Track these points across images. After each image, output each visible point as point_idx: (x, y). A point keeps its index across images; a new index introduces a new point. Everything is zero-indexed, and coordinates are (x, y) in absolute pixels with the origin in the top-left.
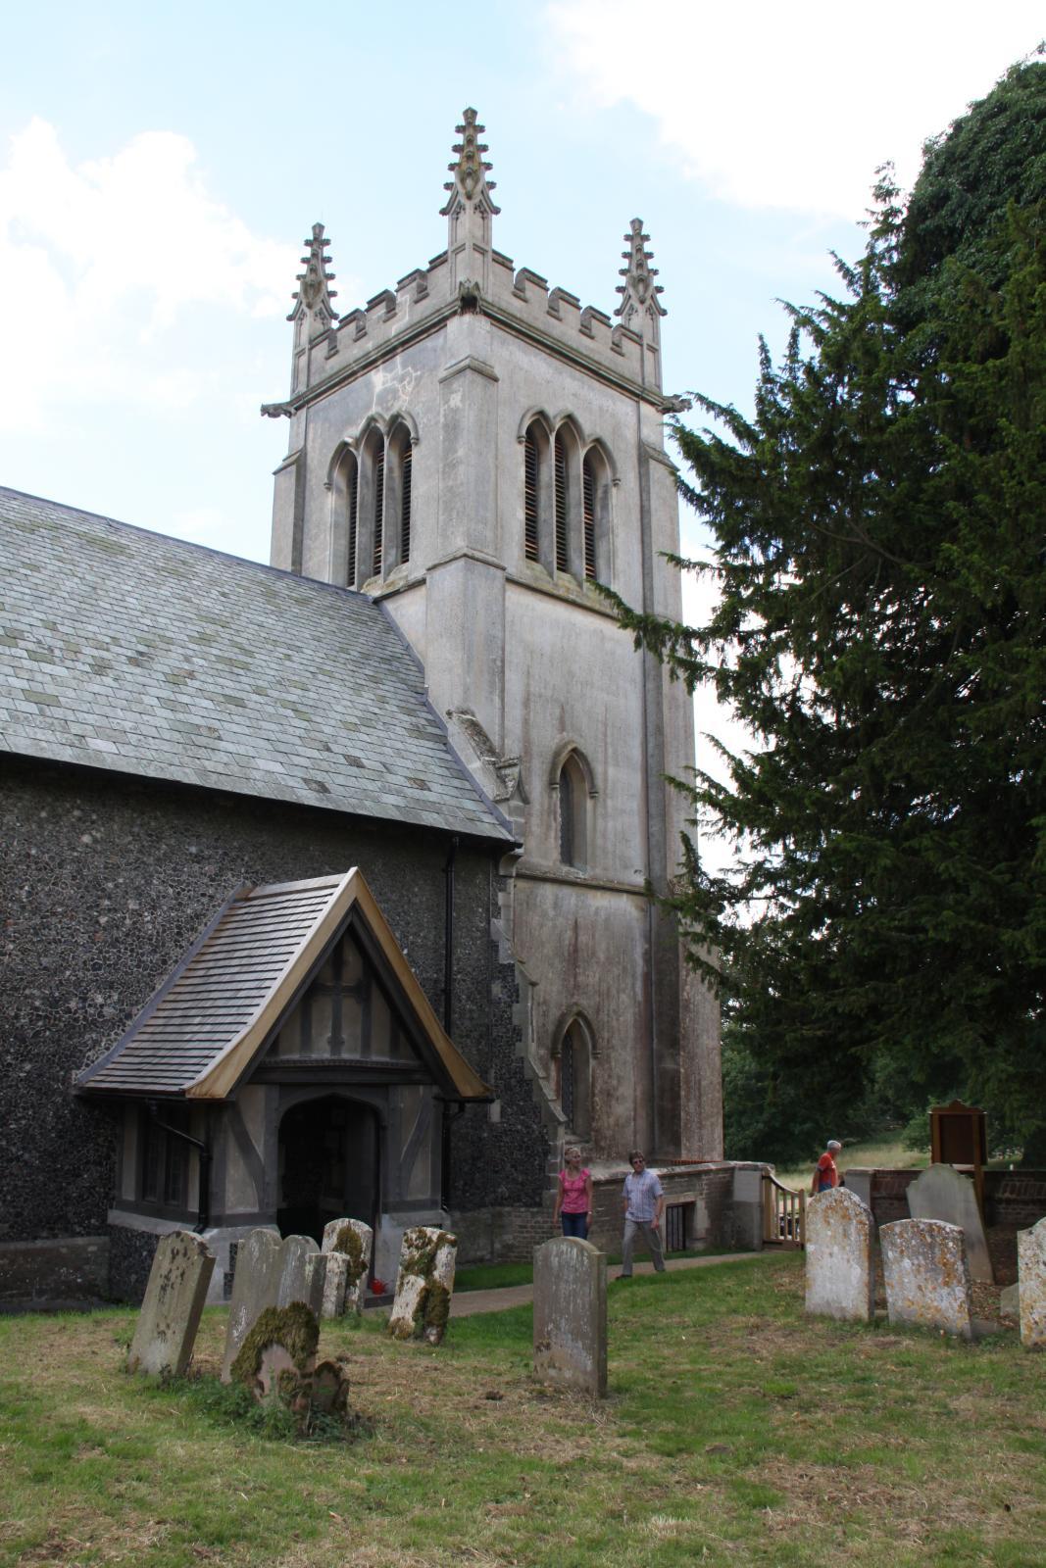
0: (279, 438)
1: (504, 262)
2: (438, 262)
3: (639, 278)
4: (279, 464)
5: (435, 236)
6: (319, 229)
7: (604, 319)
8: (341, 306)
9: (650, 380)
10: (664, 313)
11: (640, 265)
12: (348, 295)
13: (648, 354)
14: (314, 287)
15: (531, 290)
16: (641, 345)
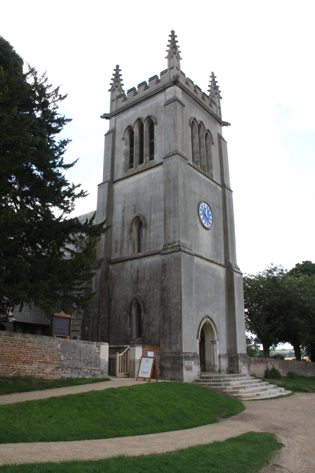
0: (106, 125)
2: (162, 73)
3: (214, 87)
4: (106, 132)
5: (164, 65)
9: (219, 116)
10: (221, 98)
11: (215, 84)
16: (216, 106)
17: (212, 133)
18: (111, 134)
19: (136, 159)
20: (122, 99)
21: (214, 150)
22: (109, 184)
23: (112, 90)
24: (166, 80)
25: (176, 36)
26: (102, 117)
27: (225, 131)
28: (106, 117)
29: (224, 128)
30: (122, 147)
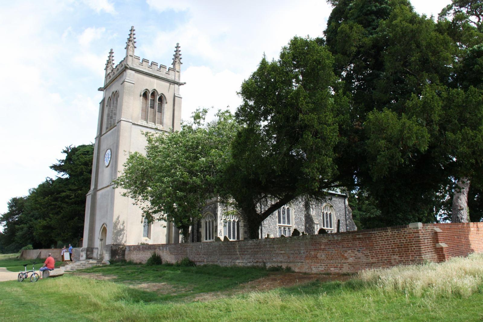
0: (101, 96)
1: (138, 58)
6: (112, 50)
13: (177, 74)
17: (165, 95)
20: (108, 77)
21: (167, 108)
27: (182, 91)
28: (100, 89)
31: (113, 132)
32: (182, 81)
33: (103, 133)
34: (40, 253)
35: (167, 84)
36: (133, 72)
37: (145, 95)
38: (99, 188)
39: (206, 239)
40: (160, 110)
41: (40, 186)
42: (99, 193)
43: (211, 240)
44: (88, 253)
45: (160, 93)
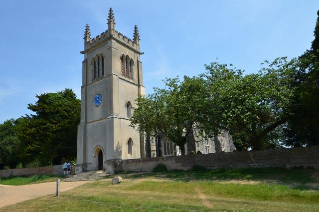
0: (82, 57)
7: (131, 40)
8: (92, 37)
12: (93, 35)
14: (87, 33)
15: (120, 36)
18: (85, 62)
19: (97, 75)
21: (135, 68)
22: (85, 87)
23: (85, 38)
24: (108, 35)
25: (112, 11)
26: (81, 53)
27: (141, 58)
28: (82, 52)
29: (141, 55)
30: (91, 68)
31: (101, 82)
32: (141, 52)
33: (88, 84)
34: (12, 172)
35: (133, 53)
36: (115, 41)
37: (122, 58)
38: (88, 121)
39: (165, 154)
40: (131, 70)
41: (5, 123)
42: (89, 126)
43: (171, 155)
44: (84, 167)
45: (130, 58)
